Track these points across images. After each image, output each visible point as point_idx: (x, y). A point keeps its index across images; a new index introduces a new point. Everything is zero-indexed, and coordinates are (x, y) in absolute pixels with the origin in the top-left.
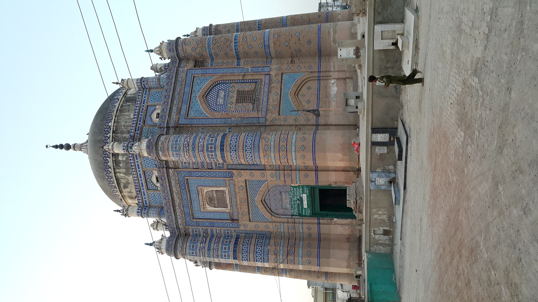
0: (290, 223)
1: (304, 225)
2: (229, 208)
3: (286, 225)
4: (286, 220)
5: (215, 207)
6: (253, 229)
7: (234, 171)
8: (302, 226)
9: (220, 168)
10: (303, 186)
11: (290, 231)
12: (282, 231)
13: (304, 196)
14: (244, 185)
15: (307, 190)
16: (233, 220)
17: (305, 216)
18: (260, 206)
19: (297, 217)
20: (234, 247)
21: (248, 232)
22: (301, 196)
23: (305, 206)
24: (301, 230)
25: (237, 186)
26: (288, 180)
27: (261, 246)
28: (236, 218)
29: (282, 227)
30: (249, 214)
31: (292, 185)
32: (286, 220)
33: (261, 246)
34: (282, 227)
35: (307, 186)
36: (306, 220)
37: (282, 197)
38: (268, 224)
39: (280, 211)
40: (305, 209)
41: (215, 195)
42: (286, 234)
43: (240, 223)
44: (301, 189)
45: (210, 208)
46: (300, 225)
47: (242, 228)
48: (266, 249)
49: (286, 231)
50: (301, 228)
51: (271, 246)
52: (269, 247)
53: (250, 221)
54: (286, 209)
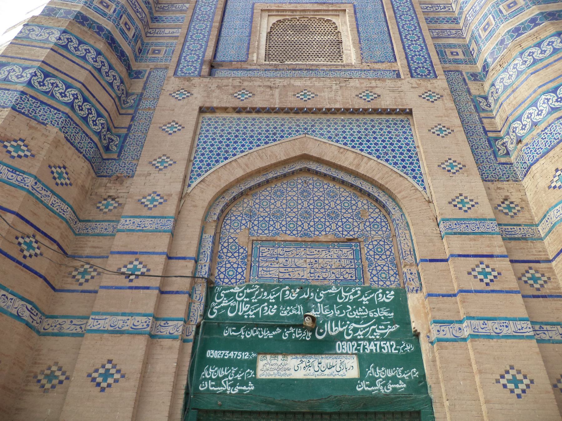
0: (166, 268)
1: (141, 342)
2: (264, 62)
3: (162, 243)
4: (187, 246)
5: (269, 34)
6: (160, 117)
7: (440, 84)
8: (135, 332)
9: (441, 54)
10: (414, 359)
11: (115, 262)
12: (125, 223)
13: (343, 367)
14: (387, 102)
15: (386, 383)
16: (213, 66)
17: (198, 363)
18: (279, 151)
19: (198, 308)
20: (100, 29)
21: (145, 104)
22: (342, 346)
23: (269, 368)
24: (105, 323)
25: (374, 84)
26: (457, 275)
27: (71, 105)
28: (220, 73)
29: (148, 224)
30: (238, 110)
31: (414, 301)
32: (187, 246)
33: (71, 105)
34: (148, 224)
35: (420, 384)
36: (170, 361)
37: (328, 245)
38: (179, 170)
39: (238, 233)
40: (253, 364)
41: (317, 38)
42: (93, 241)
43: (196, 81)
44: (389, 347)
45: (265, 25)
46: (141, 322)
47: (173, 84)
48: (51, 115)
49: (121, 242)
50: (119, 322)
51: (56, 144)
52: (54, 131)
53: (202, 110)
54: (250, 260)
